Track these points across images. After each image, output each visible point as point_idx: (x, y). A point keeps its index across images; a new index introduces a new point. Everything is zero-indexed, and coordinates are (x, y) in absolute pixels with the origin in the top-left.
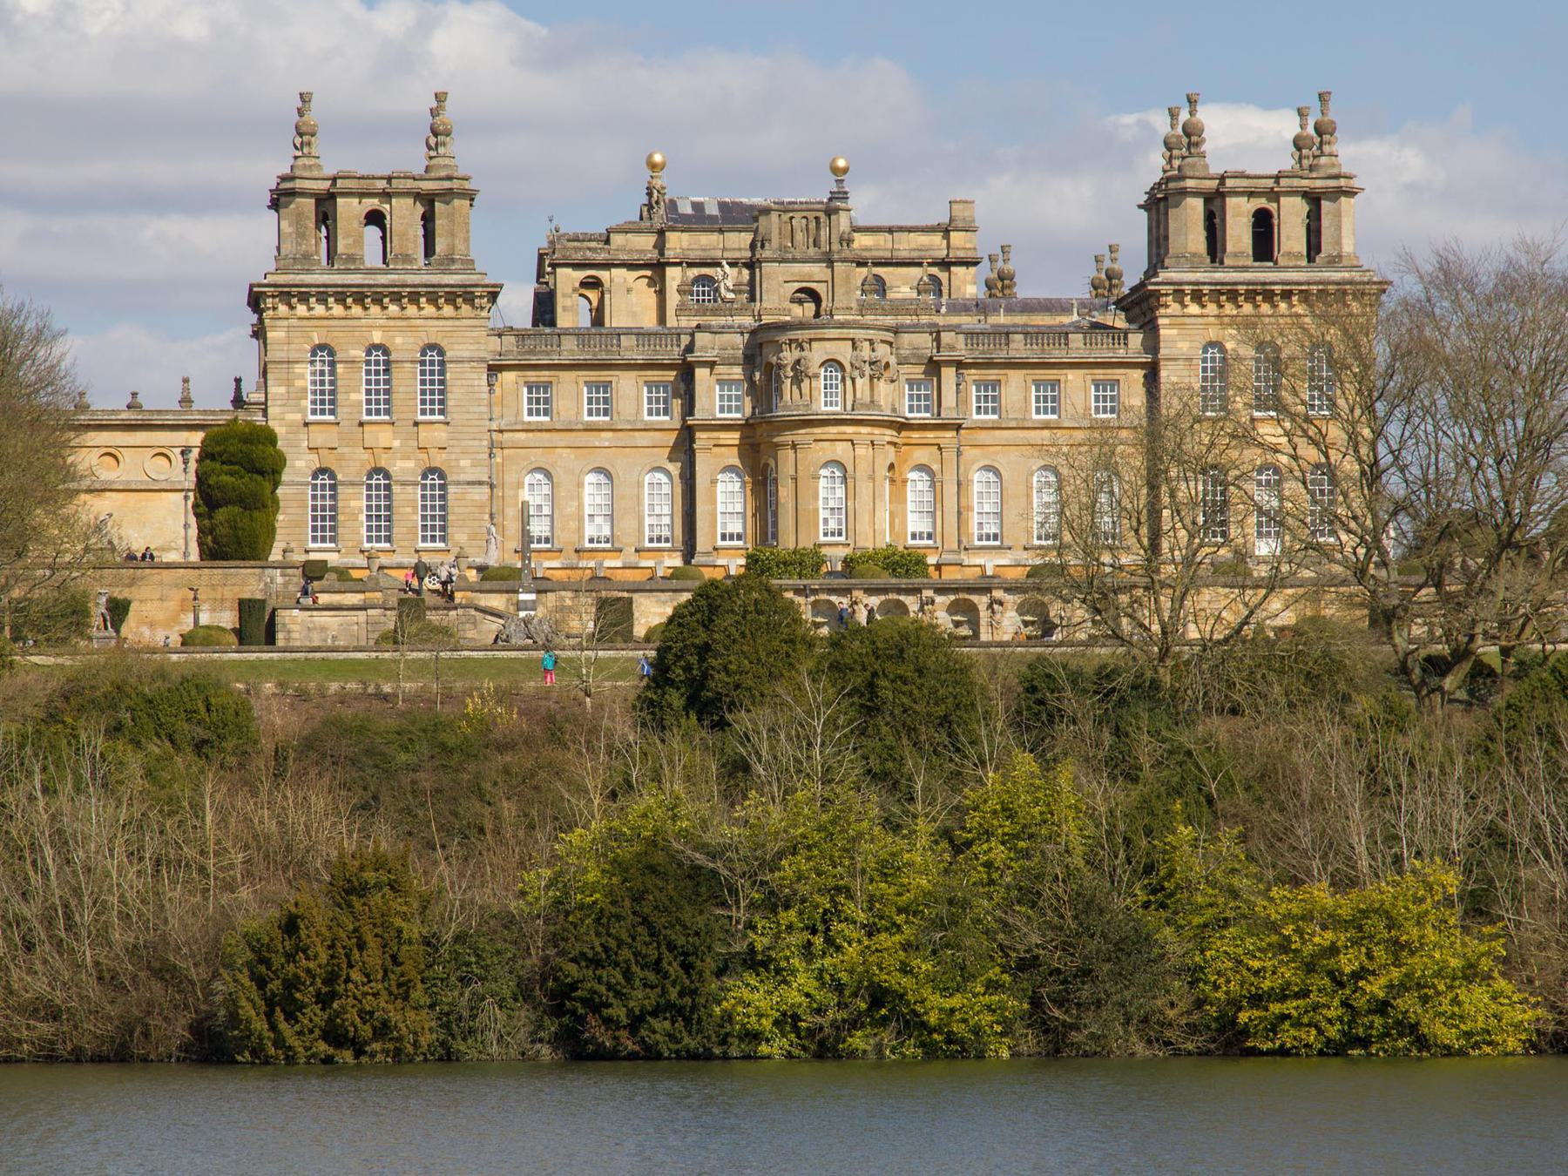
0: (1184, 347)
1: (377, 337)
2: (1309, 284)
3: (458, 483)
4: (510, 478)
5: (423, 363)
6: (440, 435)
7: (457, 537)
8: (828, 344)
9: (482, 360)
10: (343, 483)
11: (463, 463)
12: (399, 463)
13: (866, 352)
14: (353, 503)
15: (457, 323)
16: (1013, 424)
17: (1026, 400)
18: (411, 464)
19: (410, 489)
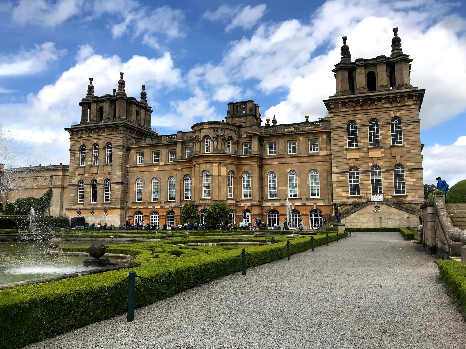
0: (340, 123)
1: (95, 142)
2: (388, 94)
3: (113, 183)
4: (132, 181)
5: (108, 149)
6: (108, 169)
7: (112, 199)
8: (206, 130)
9: (121, 146)
10: (85, 184)
11: (115, 177)
12: (99, 178)
13: (219, 133)
14: (87, 190)
15: (115, 136)
16: (280, 156)
17: (285, 148)
18: (102, 178)
19: (101, 185)
